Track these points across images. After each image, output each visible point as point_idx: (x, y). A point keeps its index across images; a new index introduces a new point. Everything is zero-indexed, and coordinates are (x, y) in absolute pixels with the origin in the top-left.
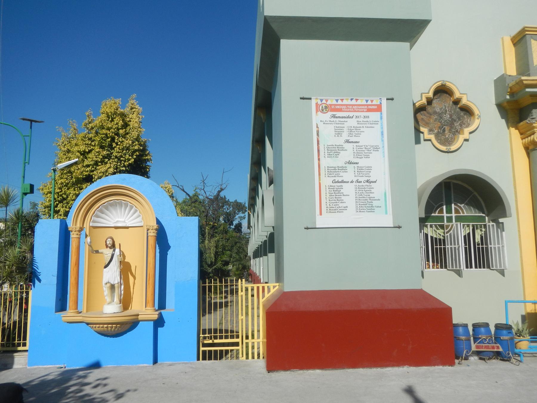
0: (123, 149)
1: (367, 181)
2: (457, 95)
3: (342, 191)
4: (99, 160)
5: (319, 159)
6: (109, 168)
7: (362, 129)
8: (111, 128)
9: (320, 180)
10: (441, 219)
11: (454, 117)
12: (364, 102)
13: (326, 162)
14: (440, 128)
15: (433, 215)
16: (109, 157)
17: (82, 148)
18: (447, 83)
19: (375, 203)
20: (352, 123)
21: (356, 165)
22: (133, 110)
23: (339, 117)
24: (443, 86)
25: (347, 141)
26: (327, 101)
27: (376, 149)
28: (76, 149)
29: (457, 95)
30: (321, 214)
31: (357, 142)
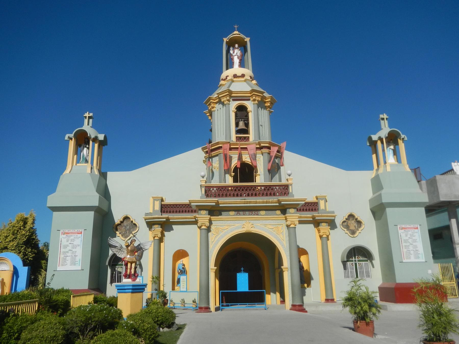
0: (22, 235)
1: (75, 256)
2: (131, 220)
3: (66, 259)
4: (11, 240)
5: (60, 249)
6: (14, 243)
7: (75, 240)
8: (17, 227)
9: (60, 255)
10: (122, 265)
11: (131, 227)
12: (77, 231)
13: (63, 250)
14: (125, 231)
15: (119, 263)
16: (16, 238)
17: (6, 235)
18: (128, 215)
19: (76, 263)
20: (72, 238)
21: (72, 251)
22: (31, 216)
23: (68, 236)
24: (126, 216)
25: (70, 244)
26: (65, 231)
27: (79, 245)
28: (3, 235)
29: (131, 220)
30: (59, 266)
31: (73, 244)
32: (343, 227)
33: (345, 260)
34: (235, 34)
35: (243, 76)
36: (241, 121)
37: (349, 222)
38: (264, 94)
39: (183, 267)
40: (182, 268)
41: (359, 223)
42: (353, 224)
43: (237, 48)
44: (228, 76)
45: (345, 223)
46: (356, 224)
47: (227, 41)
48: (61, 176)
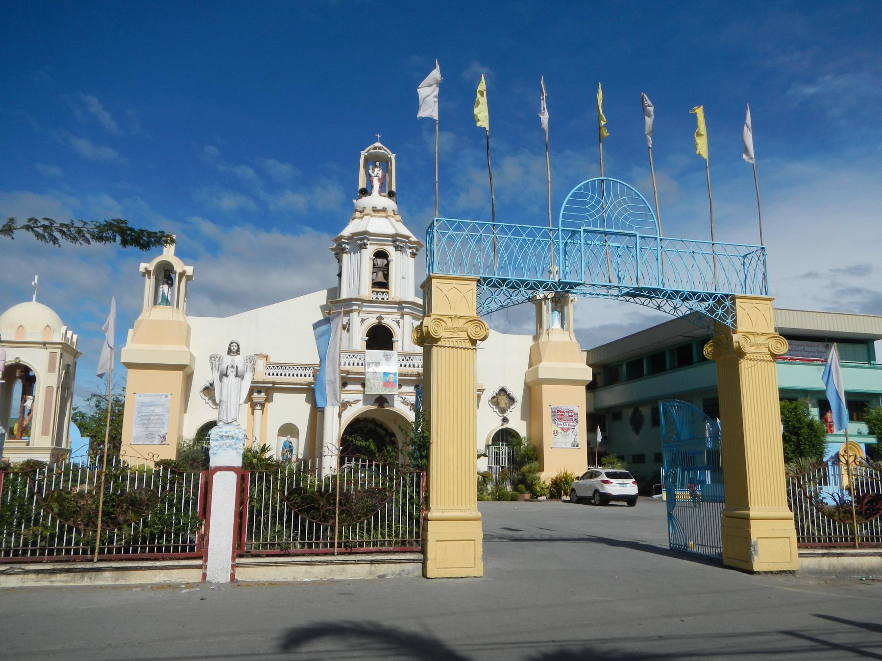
32: (492, 403)
33: (490, 443)
34: (375, 148)
35: (384, 210)
36: (381, 270)
37: (500, 397)
38: (411, 239)
39: (290, 444)
40: (288, 446)
41: (512, 400)
42: (504, 400)
43: (379, 167)
44: (365, 208)
45: (495, 399)
46: (507, 401)
47: (365, 156)
48: (136, 321)
